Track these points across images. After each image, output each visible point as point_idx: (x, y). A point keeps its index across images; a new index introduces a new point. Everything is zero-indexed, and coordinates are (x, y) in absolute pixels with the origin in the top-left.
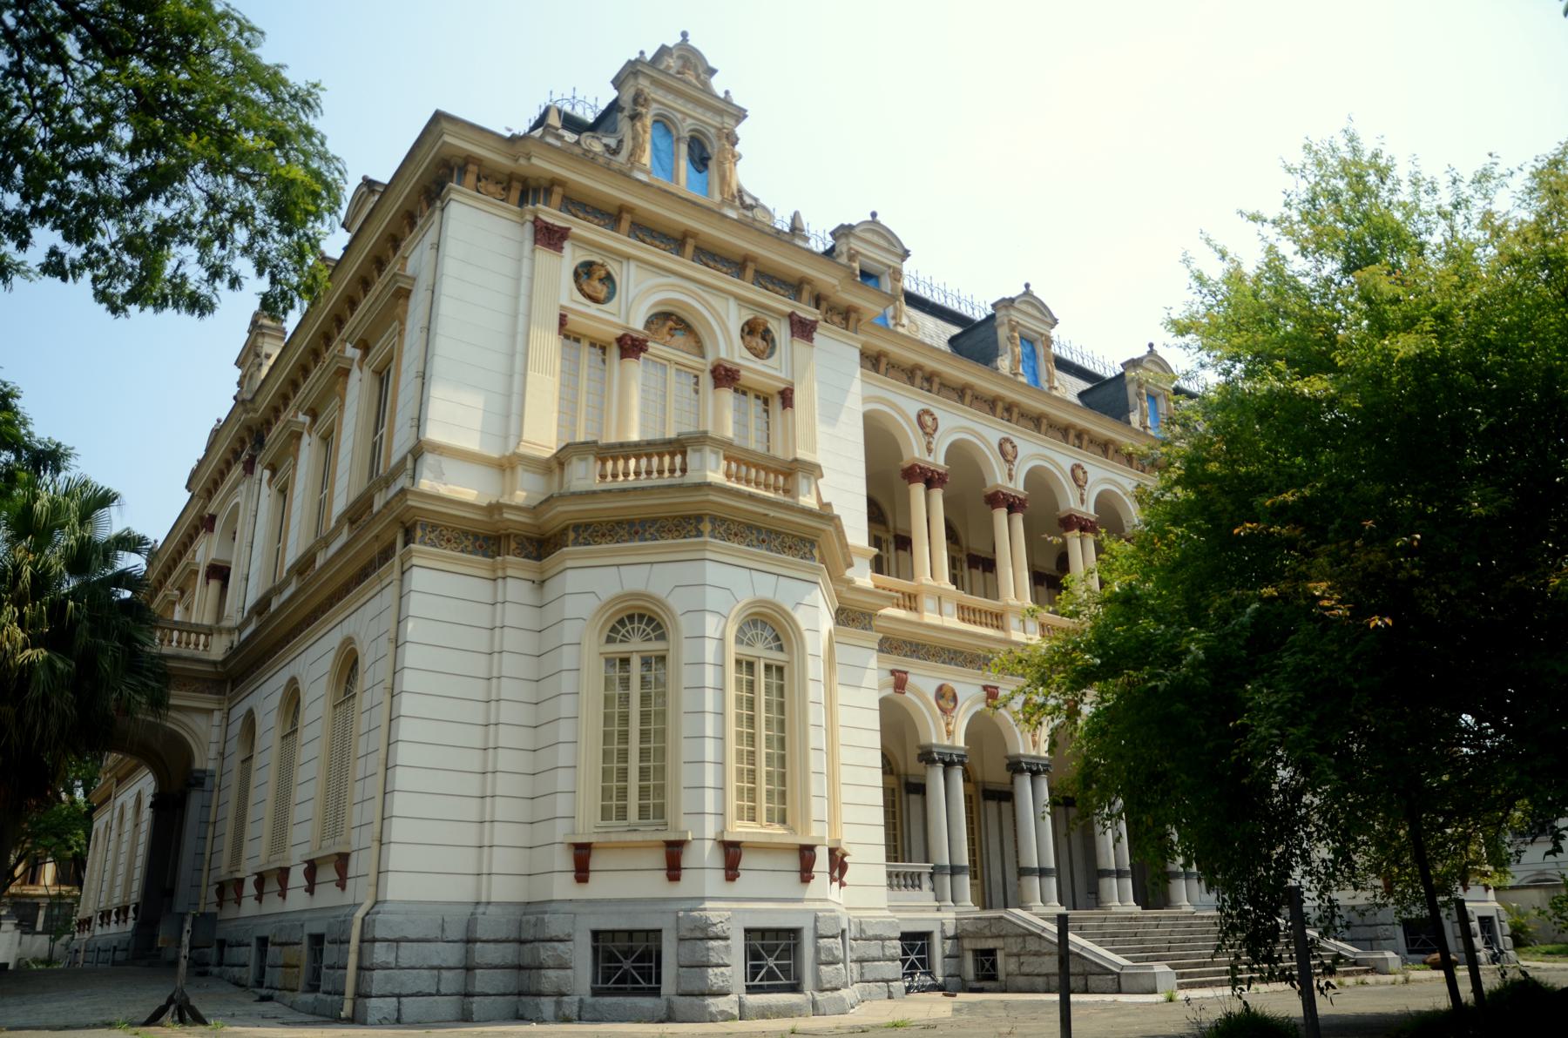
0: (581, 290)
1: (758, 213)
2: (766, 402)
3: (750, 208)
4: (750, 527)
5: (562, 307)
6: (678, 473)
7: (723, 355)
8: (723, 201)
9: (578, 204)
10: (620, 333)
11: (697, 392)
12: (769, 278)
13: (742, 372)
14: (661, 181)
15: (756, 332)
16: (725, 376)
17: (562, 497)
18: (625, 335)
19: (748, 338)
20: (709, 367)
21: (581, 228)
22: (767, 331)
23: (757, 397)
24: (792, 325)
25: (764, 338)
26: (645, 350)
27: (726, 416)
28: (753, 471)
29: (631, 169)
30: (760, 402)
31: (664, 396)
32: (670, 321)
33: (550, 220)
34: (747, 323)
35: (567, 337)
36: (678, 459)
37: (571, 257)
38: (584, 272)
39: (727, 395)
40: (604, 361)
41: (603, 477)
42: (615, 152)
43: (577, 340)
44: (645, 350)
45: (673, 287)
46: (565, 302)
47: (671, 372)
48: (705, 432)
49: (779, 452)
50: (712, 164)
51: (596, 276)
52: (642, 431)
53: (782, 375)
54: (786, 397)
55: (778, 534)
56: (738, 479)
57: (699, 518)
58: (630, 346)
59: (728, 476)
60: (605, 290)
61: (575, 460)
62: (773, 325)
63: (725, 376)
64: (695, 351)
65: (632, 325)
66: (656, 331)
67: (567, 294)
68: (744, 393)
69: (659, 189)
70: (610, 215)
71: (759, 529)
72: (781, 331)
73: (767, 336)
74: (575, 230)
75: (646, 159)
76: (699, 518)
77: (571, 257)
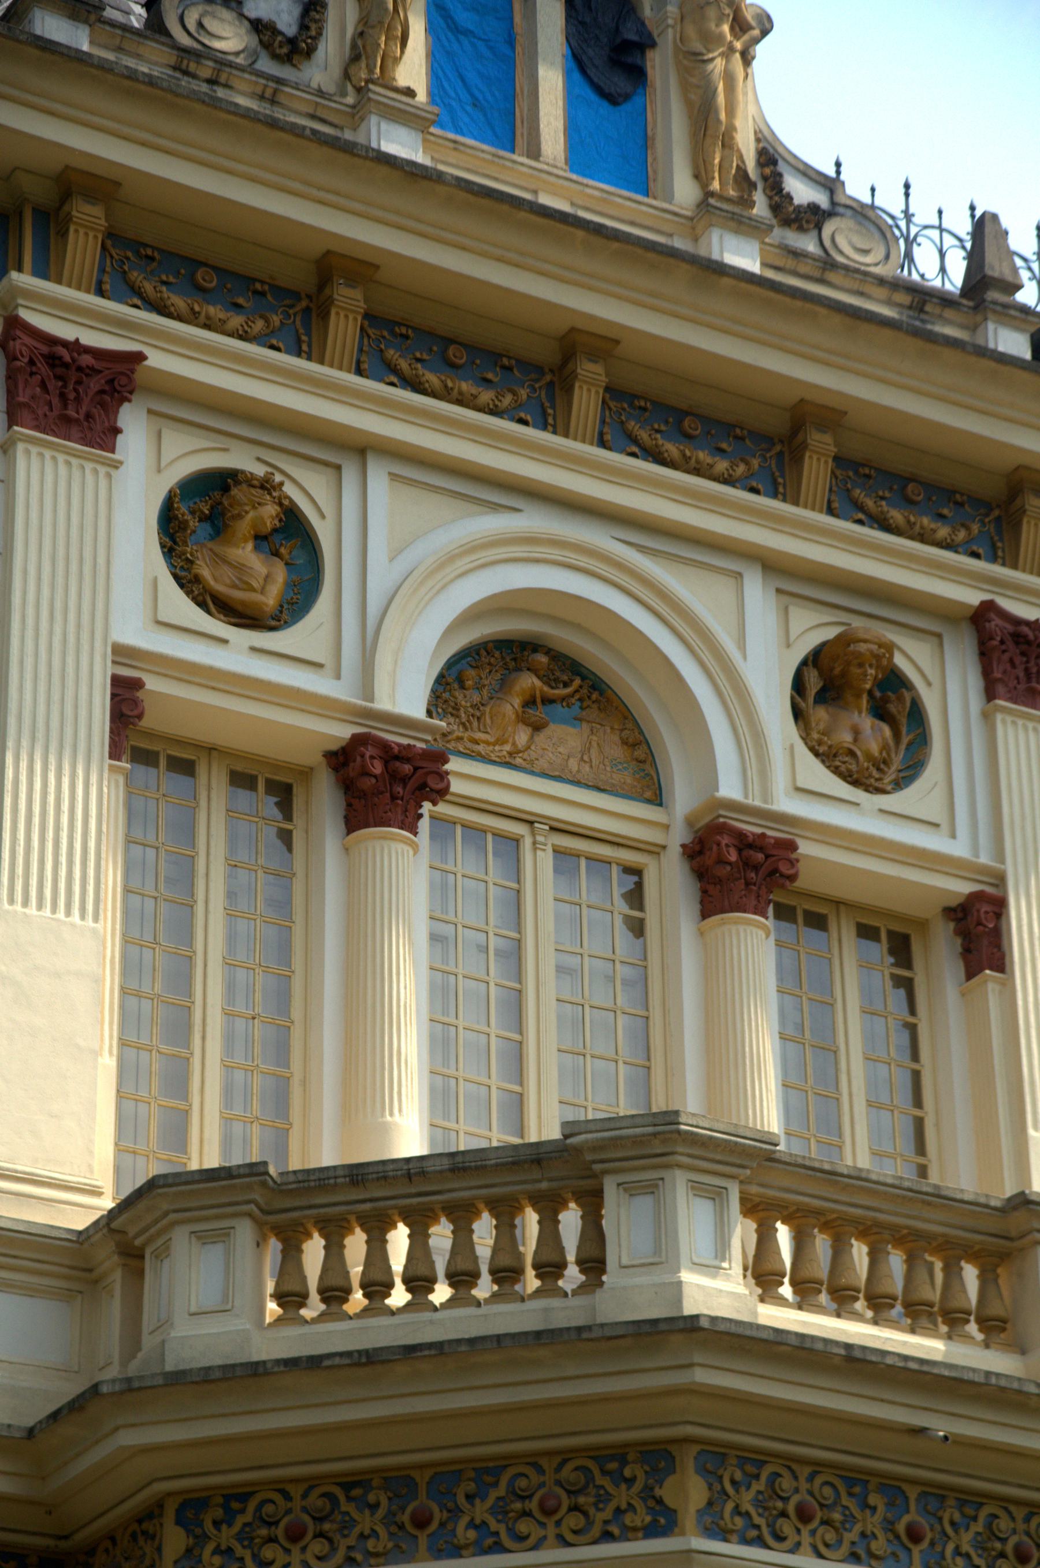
0: (188, 582)
1: (844, 239)
2: (901, 949)
3: (812, 218)
4: (856, 1481)
5: (121, 653)
6: (573, 1276)
7: (729, 789)
8: (706, 202)
9: (176, 263)
10: (343, 732)
11: (637, 928)
12: (892, 483)
13: (806, 848)
14: (473, 160)
15: (855, 702)
16: (741, 867)
17: (132, 1391)
18: (358, 740)
19: (820, 715)
20: (678, 837)
21: (180, 352)
22: (894, 682)
23: (867, 932)
24: (985, 655)
25: (880, 713)
26: (440, 793)
27: (753, 1047)
28: (859, 1252)
29: (357, 114)
30: (878, 951)
31: (514, 956)
32: (529, 673)
33: (64, 331)
34: (815, 658)
35: (144, 757)
36: (571, 1221)
37: (147, 463)
38: (198, 519)
39: (755, 944)
40: (286, 838)
41: (291, 1298)
42: (296, 49)
43: (185, 767)
44: (440, 793)
45: (529, 548)
46: (134, 632)
47: (539, 864)
48: (671, 1117)
49: (961, 1173)
50: (659, 65)
51: (244, 527)
52: (441, 1098)
53: (958, 848)
54: (978, 929)
55: (970, 1502)
56: (806, 1292)
57: (659, 1458)
58: (382, 781)
59: (764, 1276)
60: (280, 574)
61: (180, 1239)
62: (914, 658)
63: (741, 867)
64: (626, 778)
65: (383, 703)
66: (477, 716)
67: (137, 601)
68: (817, 922)
69: (462, 184)
70: (286, 295)
71: (893, 1489)
72: (946, 682)
73: (895, 703)
74: (157, 360)
75: (412, 69)
76: (659, 1458)
77: (147, 463)
